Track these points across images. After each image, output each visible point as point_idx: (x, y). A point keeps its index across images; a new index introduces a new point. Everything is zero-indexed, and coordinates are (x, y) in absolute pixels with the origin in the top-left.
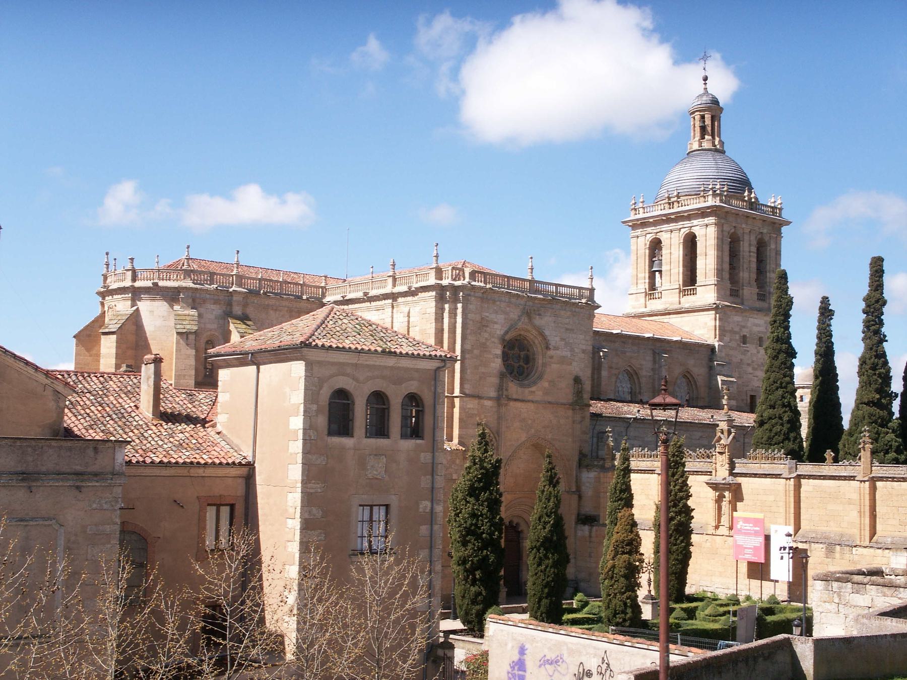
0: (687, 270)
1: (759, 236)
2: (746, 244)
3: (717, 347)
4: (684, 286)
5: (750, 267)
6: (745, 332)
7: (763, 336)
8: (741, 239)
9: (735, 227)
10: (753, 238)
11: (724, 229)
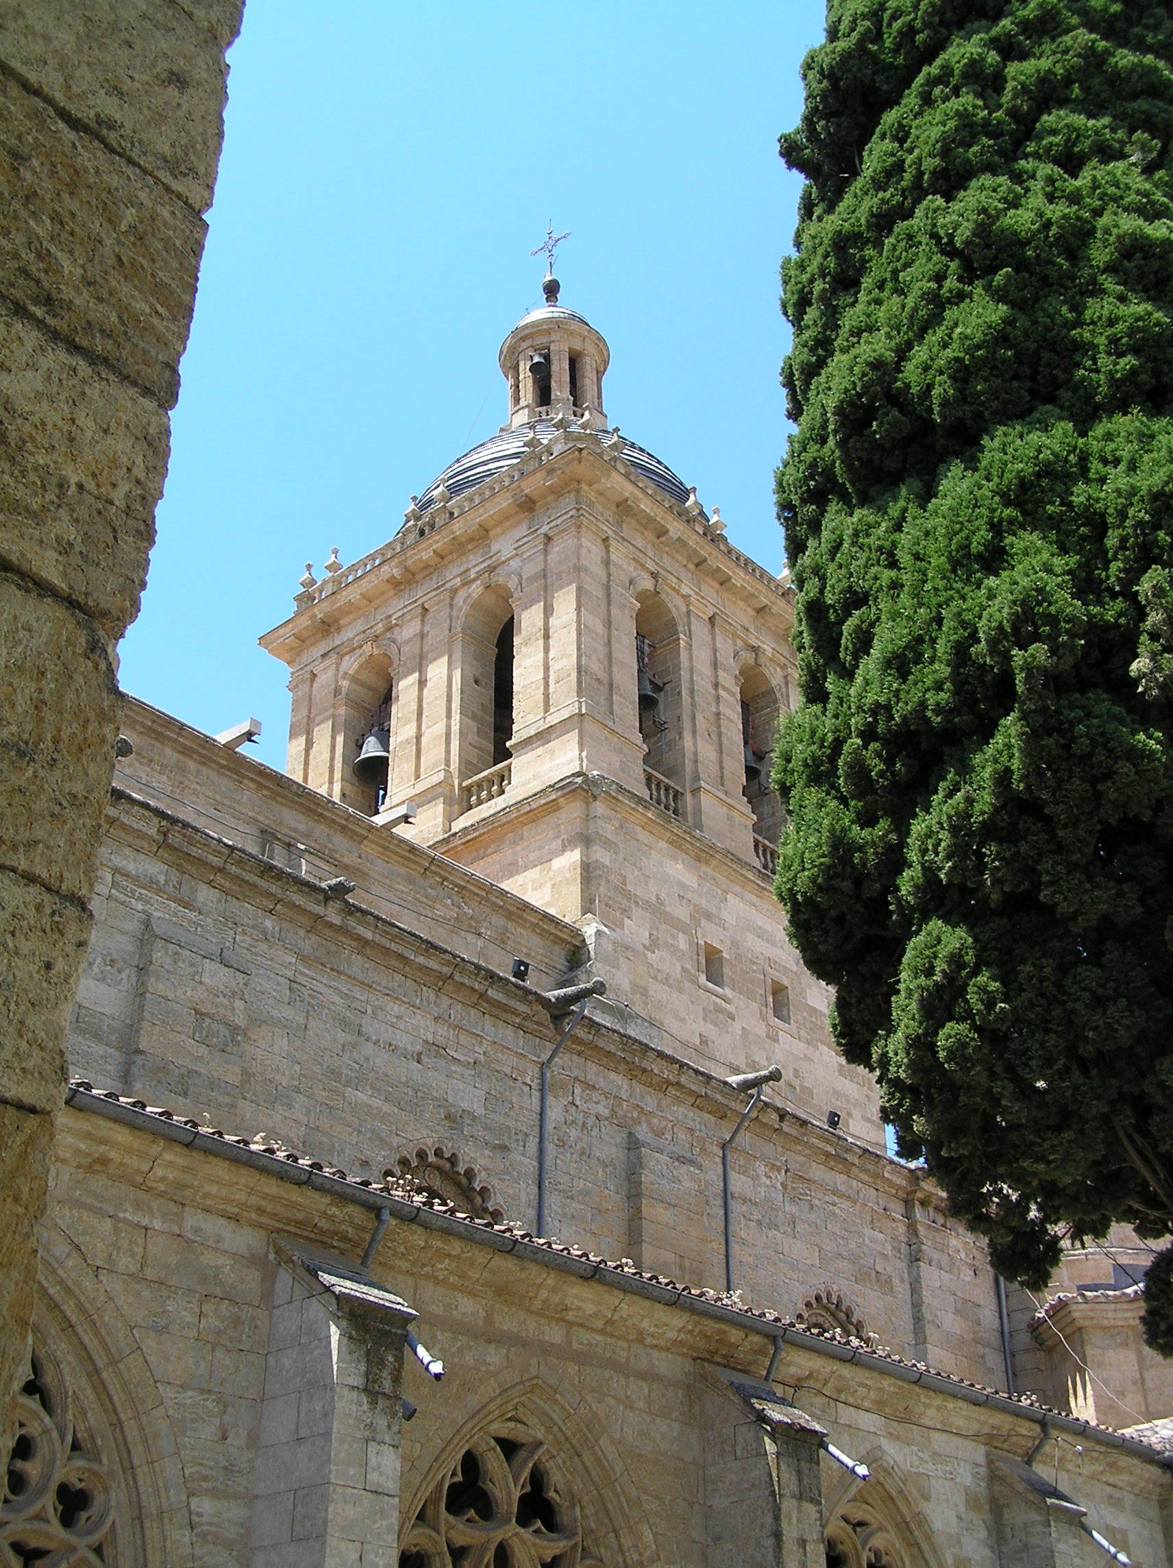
0: (480, 733)
1: (749, 658)
2: (702, 657)
3: (591, 941)
4: (463, 776)
5: (720, 734)
6: (713, 936)
7: (785, 982)
8: (680, 628)
9: (655, 576)
10: (725, 647)
11: (613, 557)
